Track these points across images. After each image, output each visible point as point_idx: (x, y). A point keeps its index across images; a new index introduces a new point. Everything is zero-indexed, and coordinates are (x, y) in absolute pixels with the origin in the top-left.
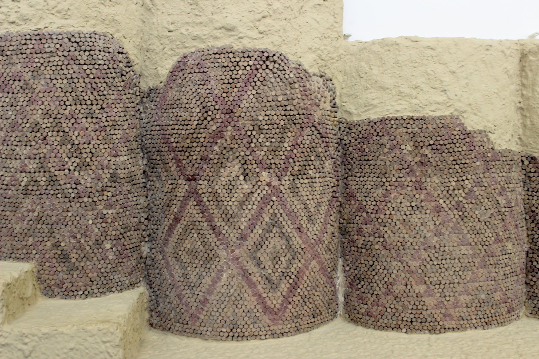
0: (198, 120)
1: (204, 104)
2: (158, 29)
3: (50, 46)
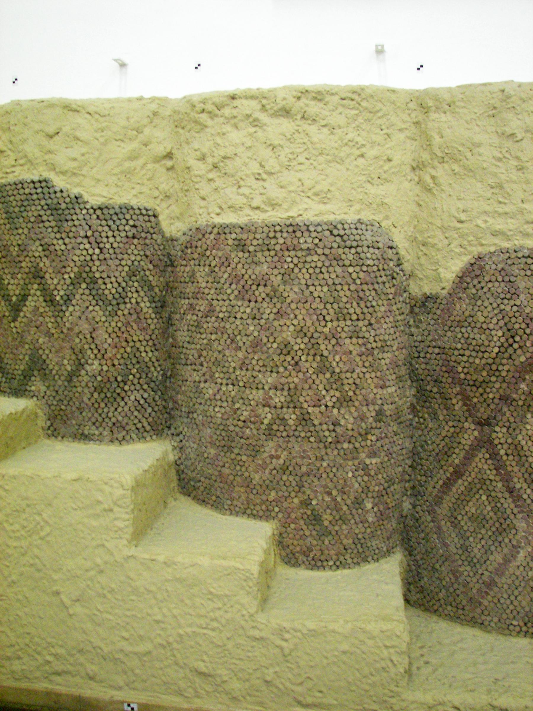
0: (499, 347)
1: (510, 326)
2: (443, 217)
3: (306, 242)
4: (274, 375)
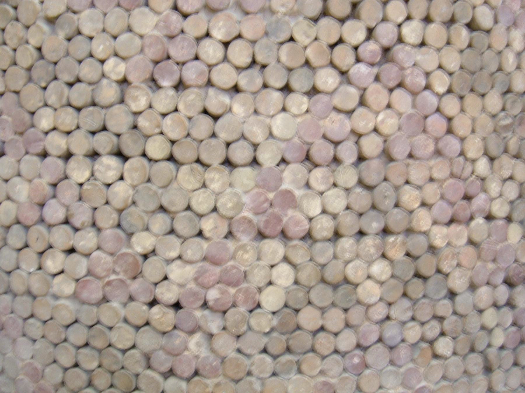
4: (298, 102)
